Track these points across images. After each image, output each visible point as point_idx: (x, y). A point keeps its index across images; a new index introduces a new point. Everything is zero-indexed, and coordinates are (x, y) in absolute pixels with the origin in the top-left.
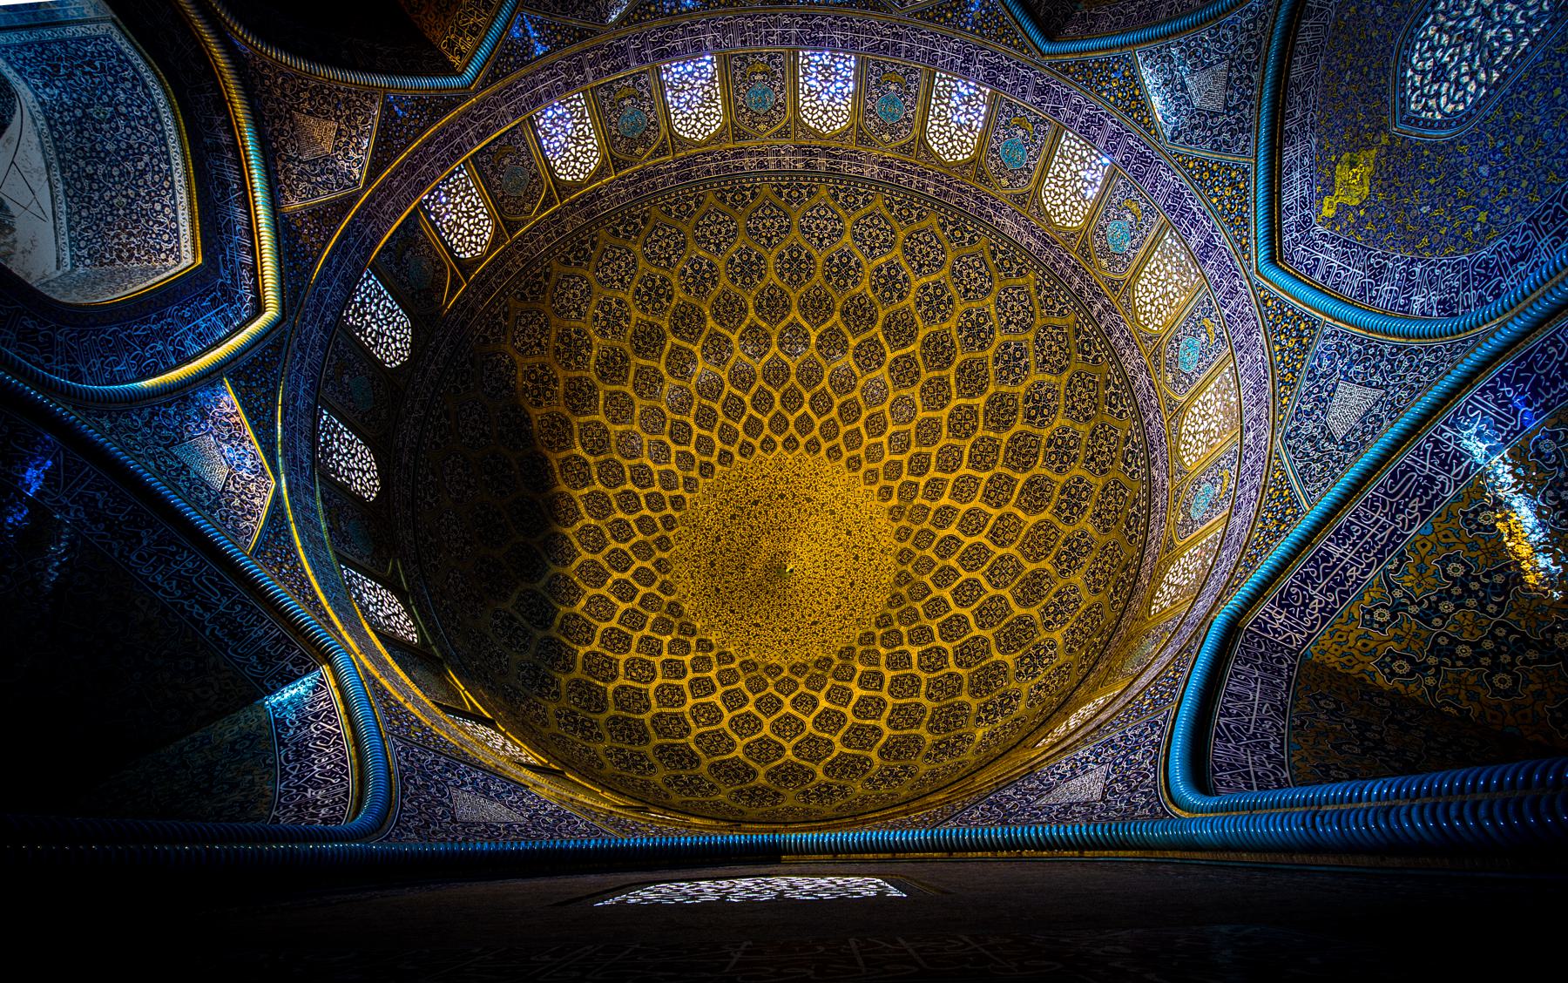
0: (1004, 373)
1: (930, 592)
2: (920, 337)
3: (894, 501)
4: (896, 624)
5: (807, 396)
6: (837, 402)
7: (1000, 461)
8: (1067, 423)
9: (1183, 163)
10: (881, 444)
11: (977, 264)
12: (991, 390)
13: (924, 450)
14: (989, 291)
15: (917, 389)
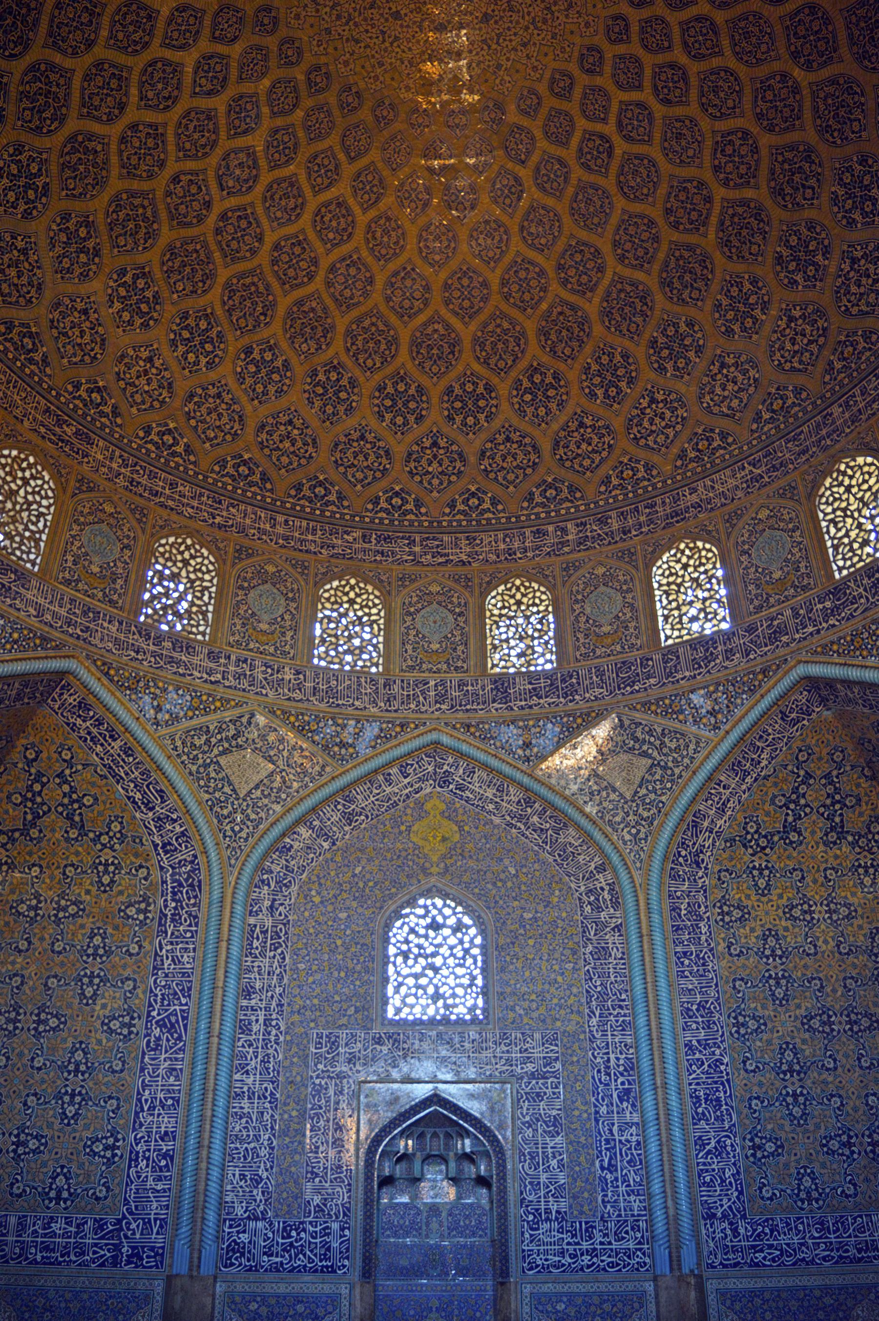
0: (605, 360)
1: (352, 160)
2: (718, 257)
3: (512, 116)
4: (309, 103)
5: (720, 17)
6: (694, 68)
7: (504, 307)
8: (496, 424)
9: (588, 714)
10: (604, 120)
11: (735, 403)
12: (598, 330)
13: (570, 191)
14: (701, 397)
15: (656, 213)
